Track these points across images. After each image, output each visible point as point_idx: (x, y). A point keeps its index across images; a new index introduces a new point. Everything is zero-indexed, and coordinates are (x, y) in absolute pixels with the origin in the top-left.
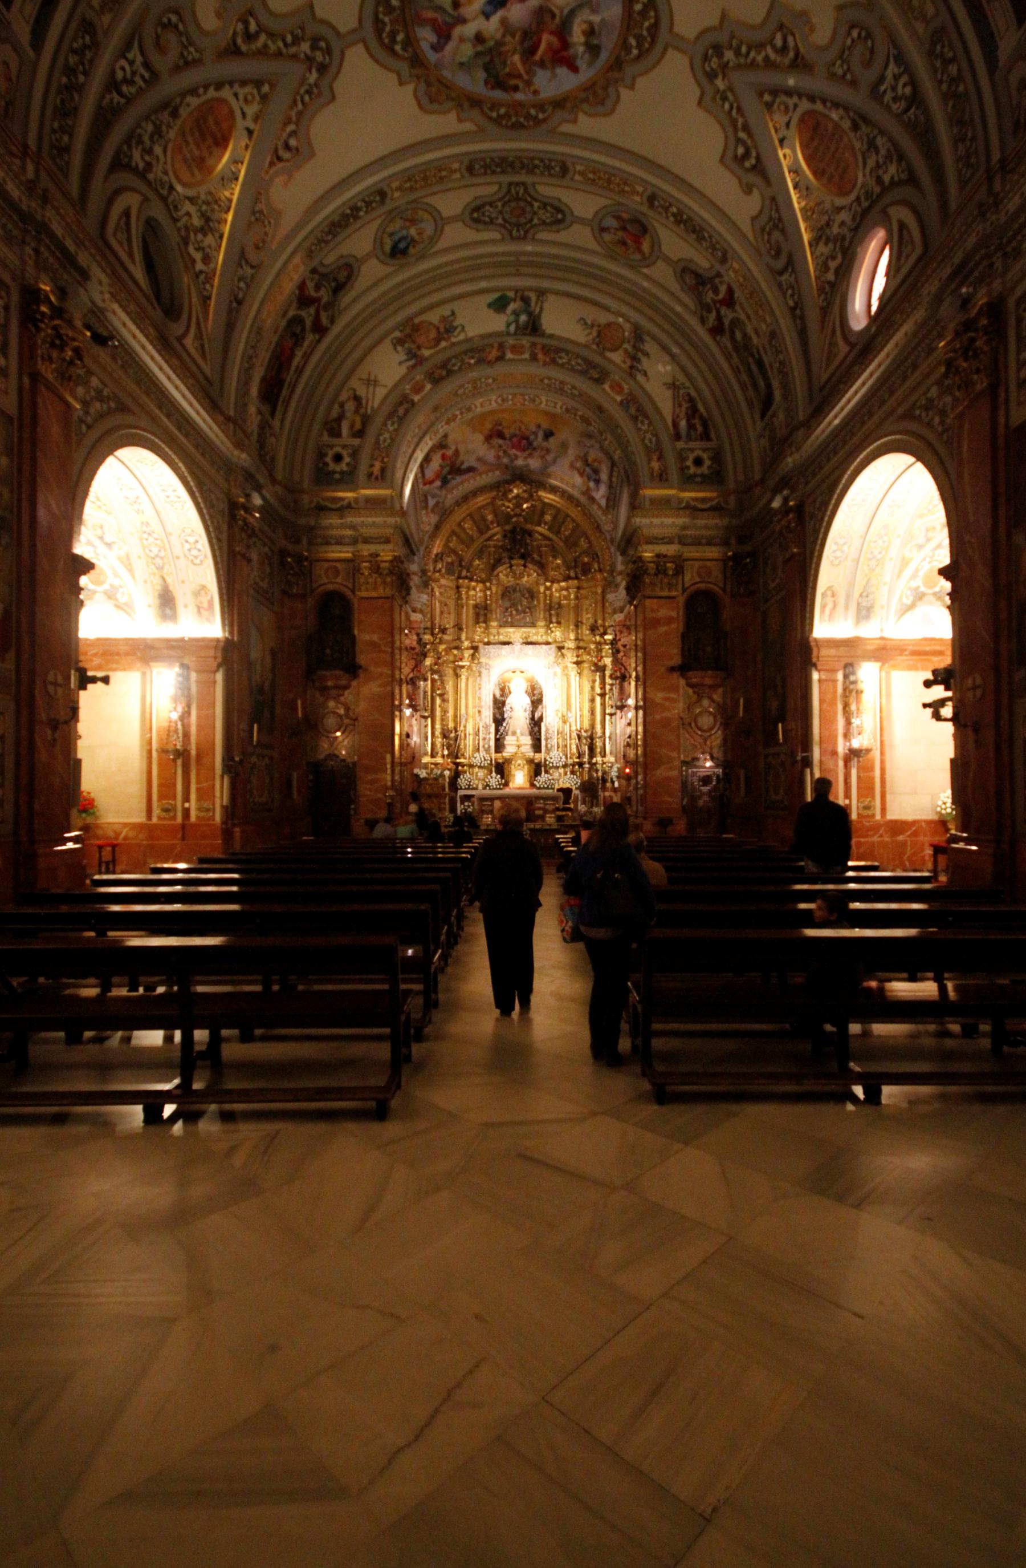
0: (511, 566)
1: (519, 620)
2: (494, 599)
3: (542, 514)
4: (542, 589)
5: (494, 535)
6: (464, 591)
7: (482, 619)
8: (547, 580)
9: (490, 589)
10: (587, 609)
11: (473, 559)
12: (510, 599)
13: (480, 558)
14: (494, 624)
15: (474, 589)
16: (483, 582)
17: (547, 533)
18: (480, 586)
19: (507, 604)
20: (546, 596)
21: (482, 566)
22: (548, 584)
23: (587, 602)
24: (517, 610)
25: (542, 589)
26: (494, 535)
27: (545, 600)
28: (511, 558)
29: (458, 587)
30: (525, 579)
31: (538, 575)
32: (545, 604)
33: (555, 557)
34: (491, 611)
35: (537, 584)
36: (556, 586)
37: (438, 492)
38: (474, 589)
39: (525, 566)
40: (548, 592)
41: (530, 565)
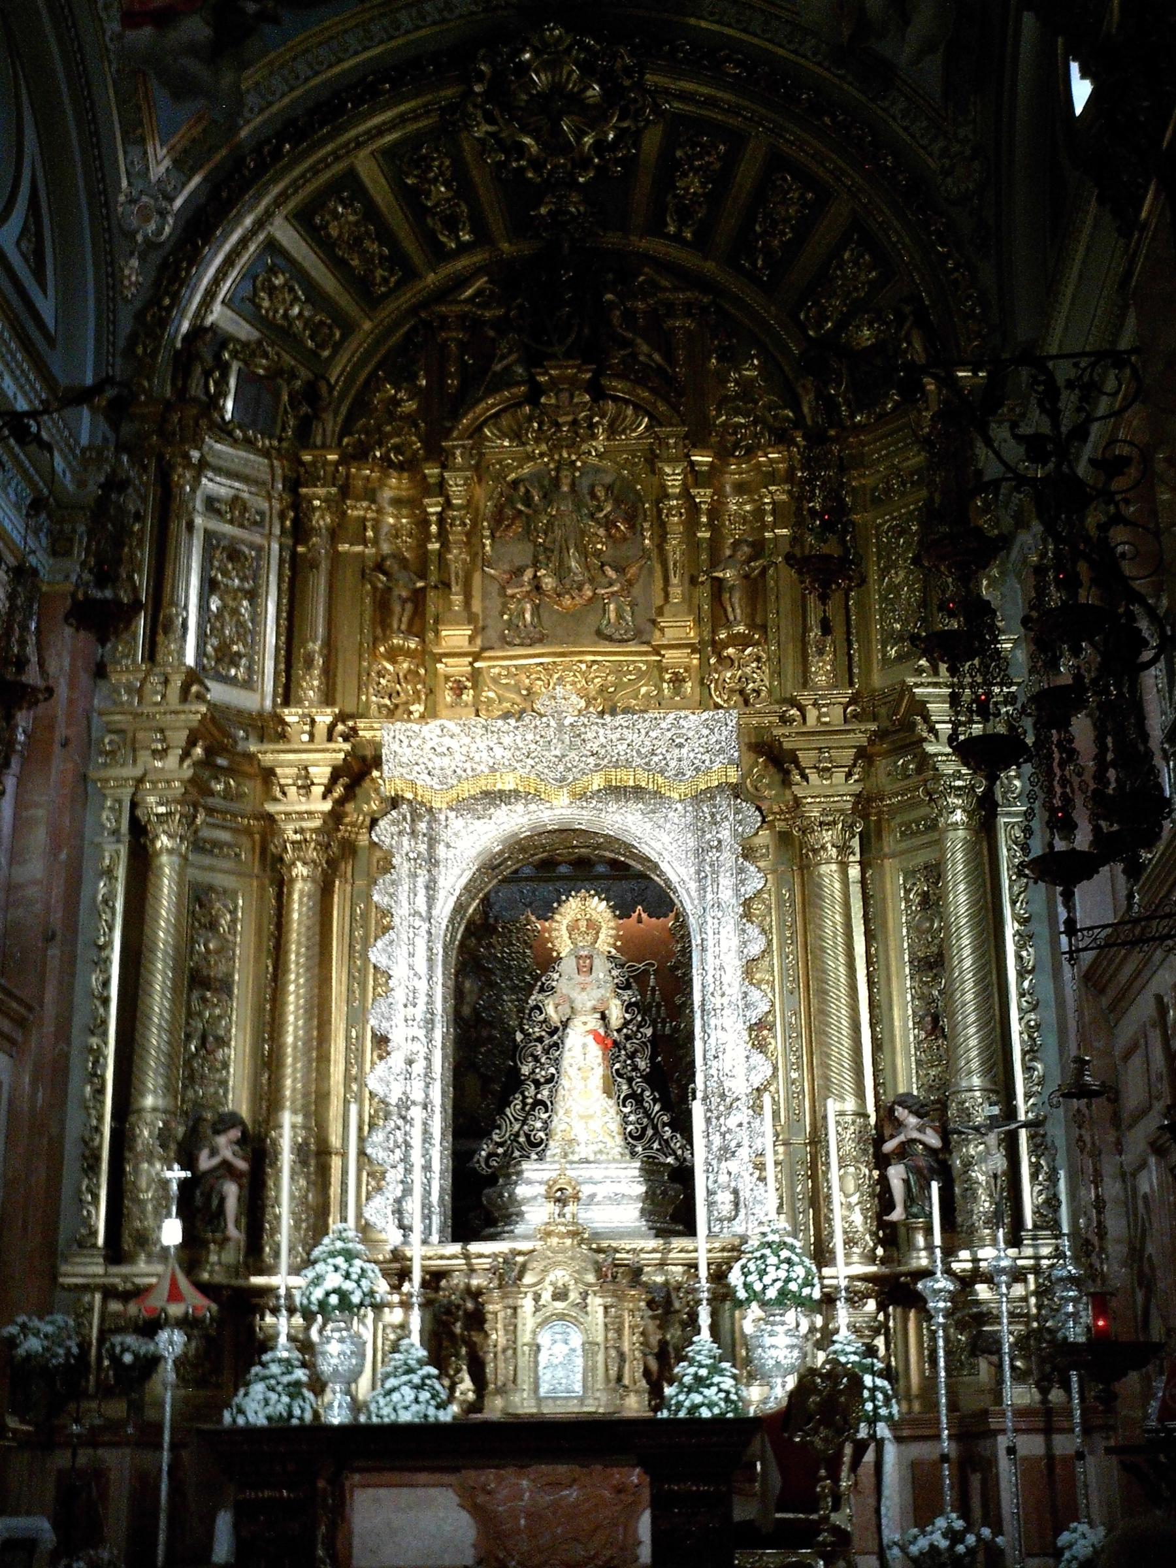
0: (534, 394)
1: (575, 617)
2: (457, 534)
3: (668, 170)
4: (674, 477)
5: (461, 281)
6: (318, 494)
7: (401, 616)
8: (697, 440)
9: (441, 487)
10: (885, 552)
11: (373, 383)
12: (528, 533)
13: (402, 375)
14: (455, 636)
15: (371, 495)
16: (410, 466)
17: (688, 259)
18: (395, 485)
19: (520, 553)
20: (694, 509)
21: (410, 406)
22: (702, 459)
23: (884, 521)
24: (561, 572)
25: (674, 477)
26: (461, 281)
27: (692, 524)
28: (534, 360)
29: (293, 485)
30: (600, 442)
31: (655, 420)
32: (693, 545)
33: (731, 358)
34: (445, 585)
35: (652, 460)
36: (735, 471)
37: (194, 66)
38: (371, 495)
39: (598, 393)
40: (703, 496)
41: (618, 387)
